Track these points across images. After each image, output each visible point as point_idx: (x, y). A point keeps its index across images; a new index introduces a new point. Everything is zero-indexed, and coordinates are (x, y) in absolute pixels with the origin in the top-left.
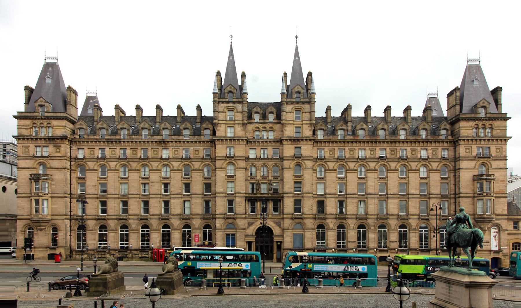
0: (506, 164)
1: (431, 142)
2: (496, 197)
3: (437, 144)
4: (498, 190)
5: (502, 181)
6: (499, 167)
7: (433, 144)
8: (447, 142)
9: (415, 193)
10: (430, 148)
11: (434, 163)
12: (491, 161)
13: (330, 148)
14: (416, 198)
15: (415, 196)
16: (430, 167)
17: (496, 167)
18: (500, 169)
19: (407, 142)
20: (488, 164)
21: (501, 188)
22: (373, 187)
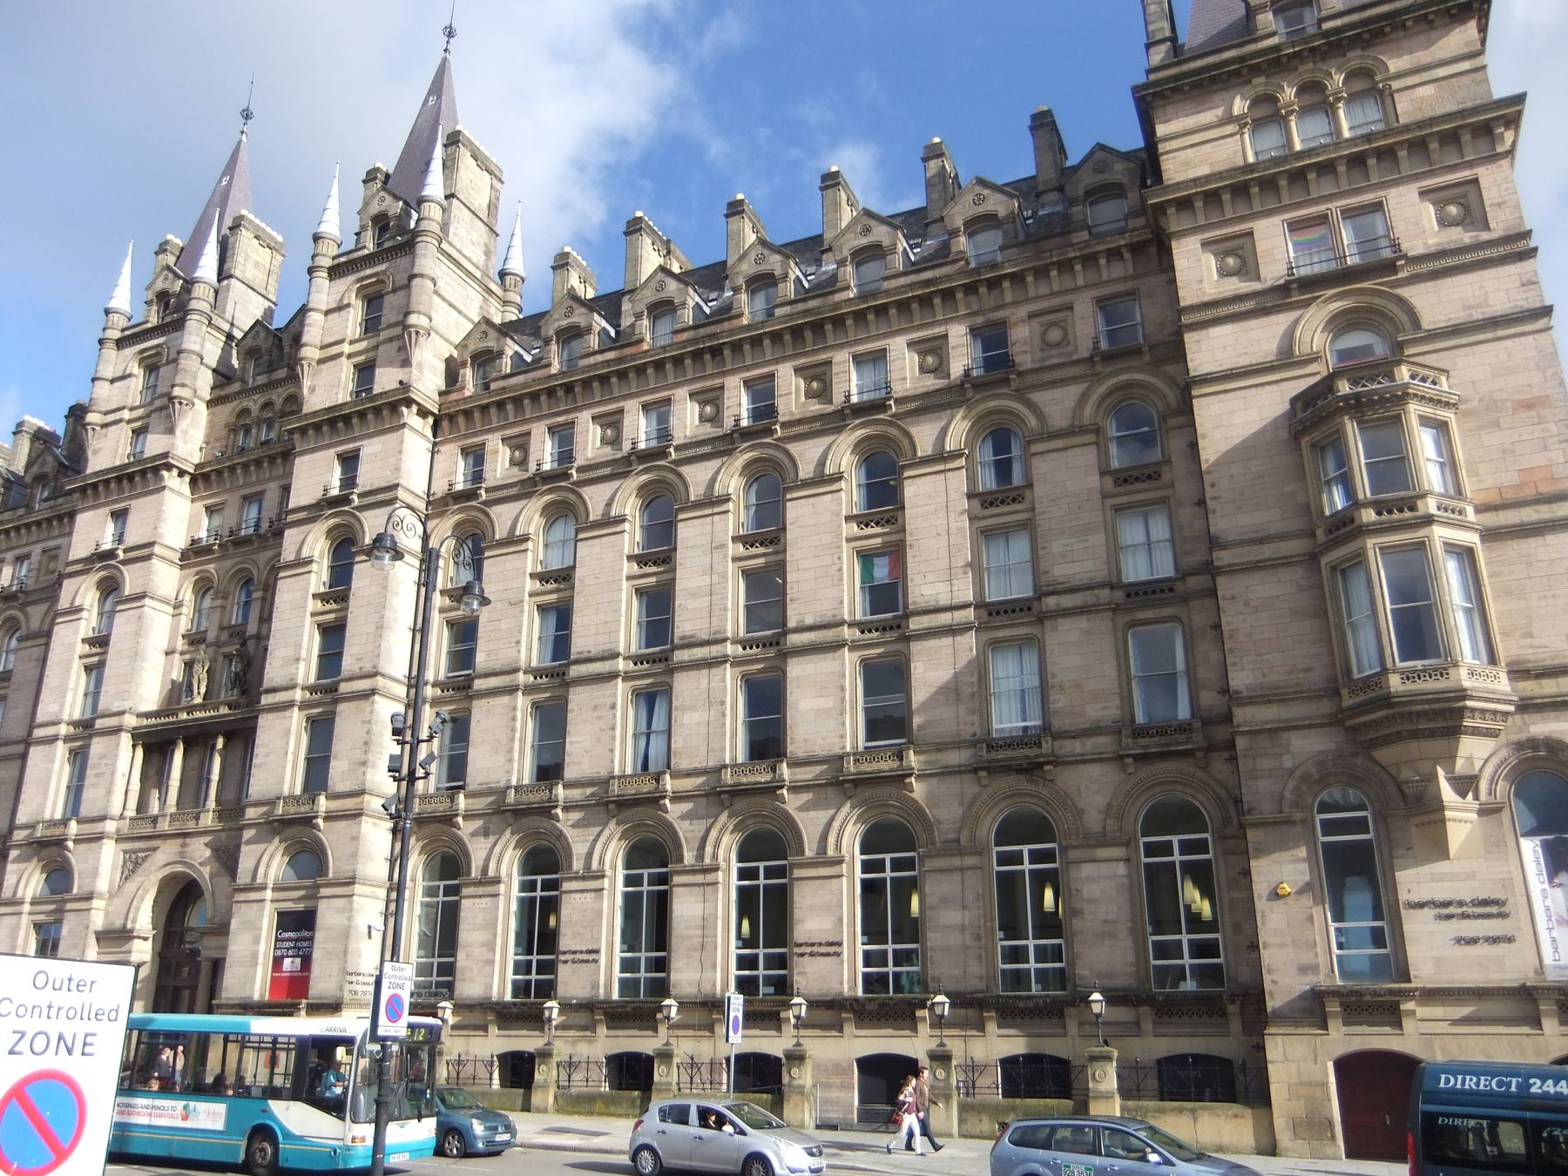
0: (1530, 283)
1: (1018, 278)
2: (1491, 535)
3: (1056, 280)
4: (1509, 478)
5: (1528, 405)
6: (1478, 315)
7: (1034, 287)
8: (1114, 254)
9: (944, 601)
10: (1023, 311)
11: (1057, 393)
12: (1404, 292)
13: (509, 432)
14: (952, 630)
15: (945, 618)
16: (1032, 422)
17: (1459, 316)
18: (1494, 323)
19: (881, 311)
20: (1392, 307)
21: (1538, 460)
22: (704, 602)
